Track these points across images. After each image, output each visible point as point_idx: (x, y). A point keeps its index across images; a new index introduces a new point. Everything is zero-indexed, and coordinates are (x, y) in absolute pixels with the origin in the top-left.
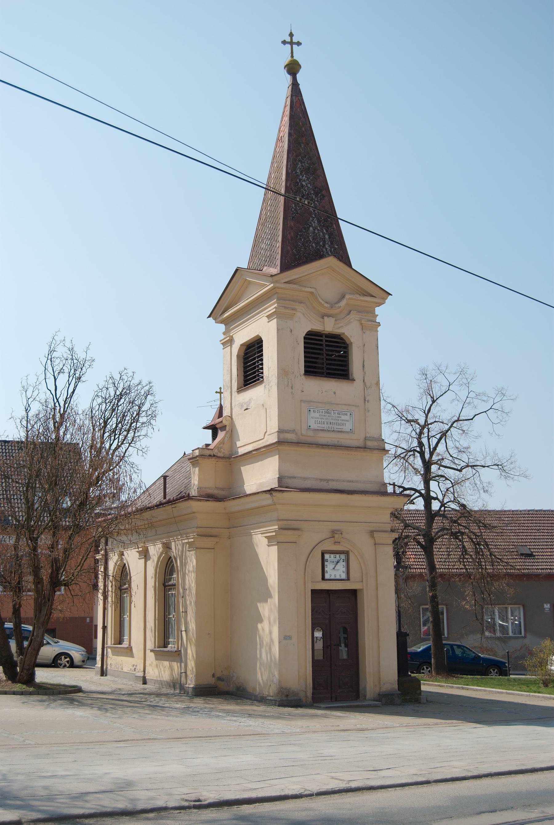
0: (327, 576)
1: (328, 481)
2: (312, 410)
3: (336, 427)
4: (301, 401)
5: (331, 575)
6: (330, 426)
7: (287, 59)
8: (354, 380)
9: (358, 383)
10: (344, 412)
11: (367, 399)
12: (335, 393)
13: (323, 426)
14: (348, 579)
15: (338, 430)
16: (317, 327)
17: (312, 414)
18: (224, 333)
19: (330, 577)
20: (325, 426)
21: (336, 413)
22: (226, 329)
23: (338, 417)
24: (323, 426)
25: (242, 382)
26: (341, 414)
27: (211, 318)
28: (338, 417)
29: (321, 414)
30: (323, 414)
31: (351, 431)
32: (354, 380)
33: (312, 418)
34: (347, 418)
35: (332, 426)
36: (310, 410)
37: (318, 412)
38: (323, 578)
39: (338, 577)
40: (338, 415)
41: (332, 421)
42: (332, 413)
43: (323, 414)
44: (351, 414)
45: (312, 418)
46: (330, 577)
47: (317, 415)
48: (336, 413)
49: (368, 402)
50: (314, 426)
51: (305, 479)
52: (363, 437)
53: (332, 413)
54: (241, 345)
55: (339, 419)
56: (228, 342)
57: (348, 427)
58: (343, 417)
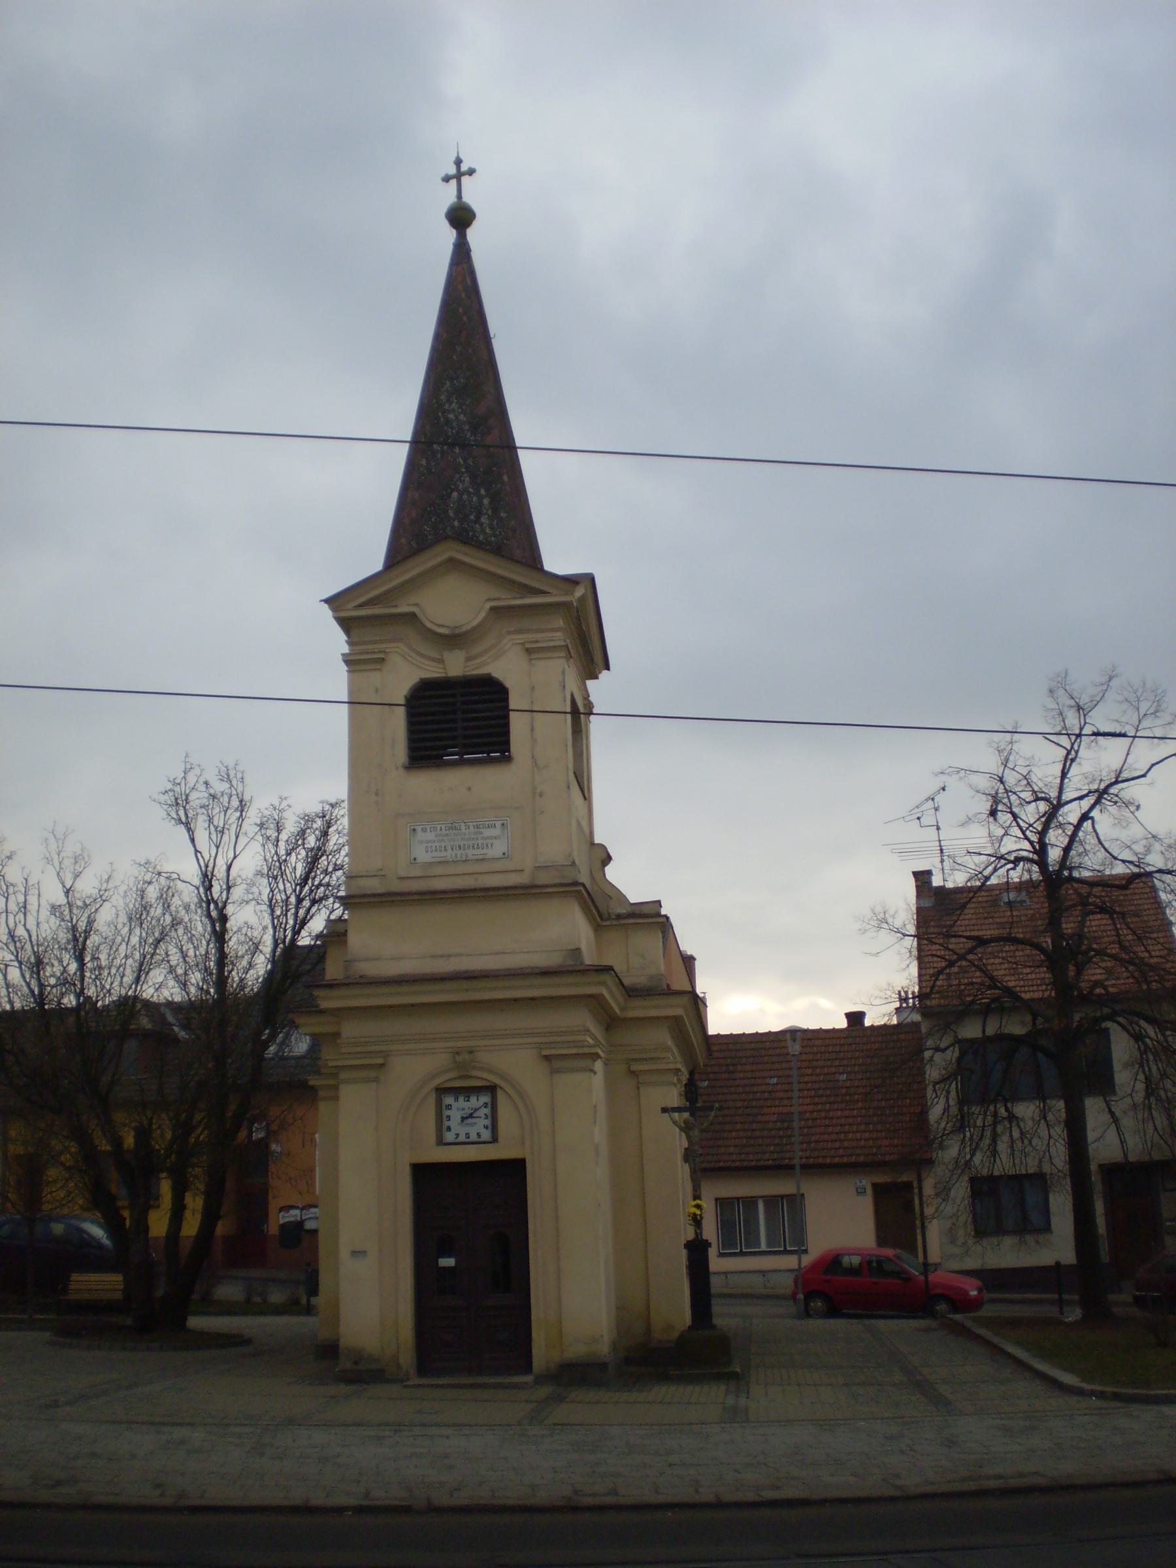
0: (449, 1137)
2: (419, 829)
3: (471, 853)
5: (457, 1135)
6: (459, 852)
7: (447, 196)
10: (487, 823)
11: (538, 791)
12: (469, 789)
13: (443, 854)
14: (495, 1139)
15: (476, 857)
16: (433, 672)
17: (420, 835)
19: (456, 1138)
20: (449, 855)
21: (472, 828)
23: (476, 834)
24: (443, 854)
26: (481, 826)
28: (476, 834)
29: (439, 832)
30: (444, 832)
33: (421, 842)
34: (496, 832)
35: (462, 851)
36: (414, 830)
37: (432, 829)
38: (441, 1142)
39: (474, 1137)
40: (476, 830)
41: (462, 843)
42: (463, 827)
44: (503, 824)
45: (421, 842)
46: (456, 1138)
47: (430, 836)
48: (472, 828)
49: (541, 796)
50: (422, 856)
53: (463, 827)
55: (479, 836)
58: (487, 833)
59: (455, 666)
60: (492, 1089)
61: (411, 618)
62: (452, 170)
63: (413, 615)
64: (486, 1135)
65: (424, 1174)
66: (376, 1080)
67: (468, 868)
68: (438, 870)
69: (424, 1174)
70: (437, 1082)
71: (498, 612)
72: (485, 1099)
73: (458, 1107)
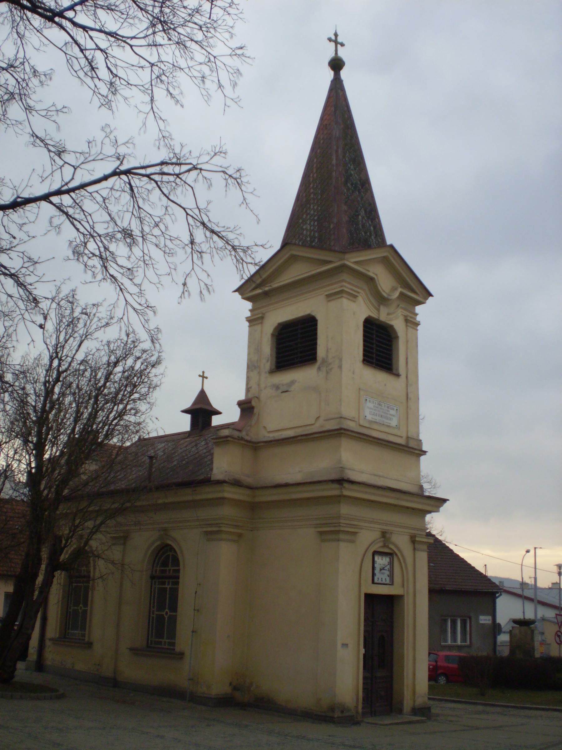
2: (368, 400)
4: (359, 389)
12: (385, 385)
14: (392, 584)
16: (374, 315)
18: (251, 311)
20: (378, 419)
22: (253, 306)
27: (237, 293)
30: (376, 405)
36: (366, 400)
38: (373, 582)
39: (384, 582)
43: (376, 405)
50: (369, 417)
52: (404, 435)
53: (383, 405)
54: (280, 324)
57: (394, 423)
62: (340, 40)
63: (372, 279)
66: (352, 541)
67: (387, 430)
68: (375, 426)
70: (375, 548)
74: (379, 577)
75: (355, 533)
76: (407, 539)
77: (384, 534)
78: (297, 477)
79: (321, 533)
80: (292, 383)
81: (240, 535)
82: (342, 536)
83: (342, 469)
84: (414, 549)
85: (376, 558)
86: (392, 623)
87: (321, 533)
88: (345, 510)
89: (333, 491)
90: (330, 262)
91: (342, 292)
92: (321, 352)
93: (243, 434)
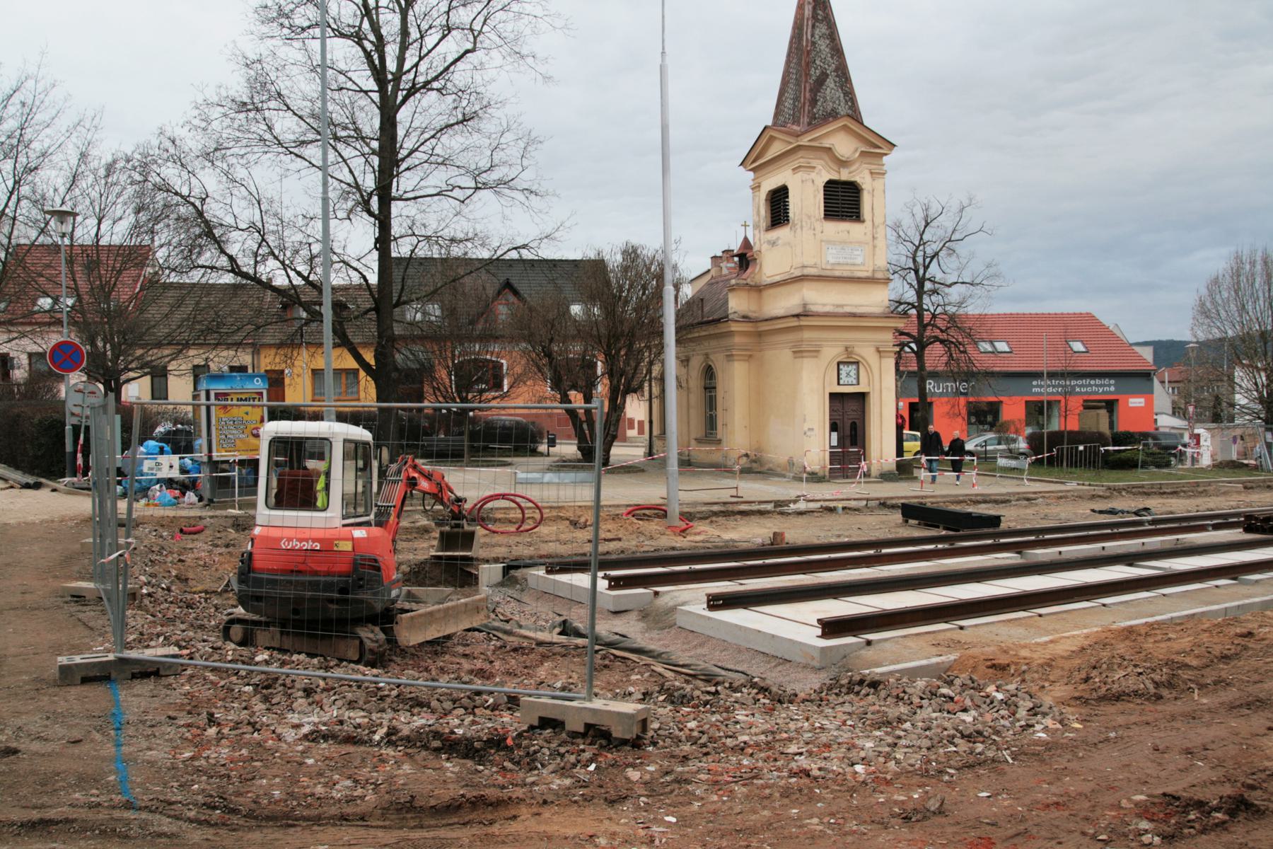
0: (841, 382)
1: (842, 306)
8: (863, 221)
9: (868, 223)
16: (835, 177)
17: (830, 251)
20: (841, 261)
25: (769, 223)
31: (863, 264)
32: (863, 221)
38: (839, 384)
47: (834, 251)
50: (832, 261)
51: (824, 305)
52: (871, 269)
56: (756, 188)
57: (859, 260)
58: (856, 253)
59: (845, 176)
60: (857, 363)
61: (829, 150)
63: (830, 149)
64: (855, 382)
65: (834, 397)
68: (837, 267)
69: (834, 397)
70: (839, 360)
71: (863, 153)
72: (854, 367)
73: (844, 369)
74: (844, 379)
75: (818, 351)
76: (873, 350)
77: (847, 349)
78: (779, 311)
79: (794, 352)
80: (778, 238)
81: (750, 356)
82: (805, 354)
83: (805, 305)
84: (880, 357)
85: (841, 367)
86: (864, 412)
87: (794, 352)
88: (807, 335)
89: (794, 323)
90: (790, 143)
91: (800, 167)
92: (791, 215)
93: (749, 281)
